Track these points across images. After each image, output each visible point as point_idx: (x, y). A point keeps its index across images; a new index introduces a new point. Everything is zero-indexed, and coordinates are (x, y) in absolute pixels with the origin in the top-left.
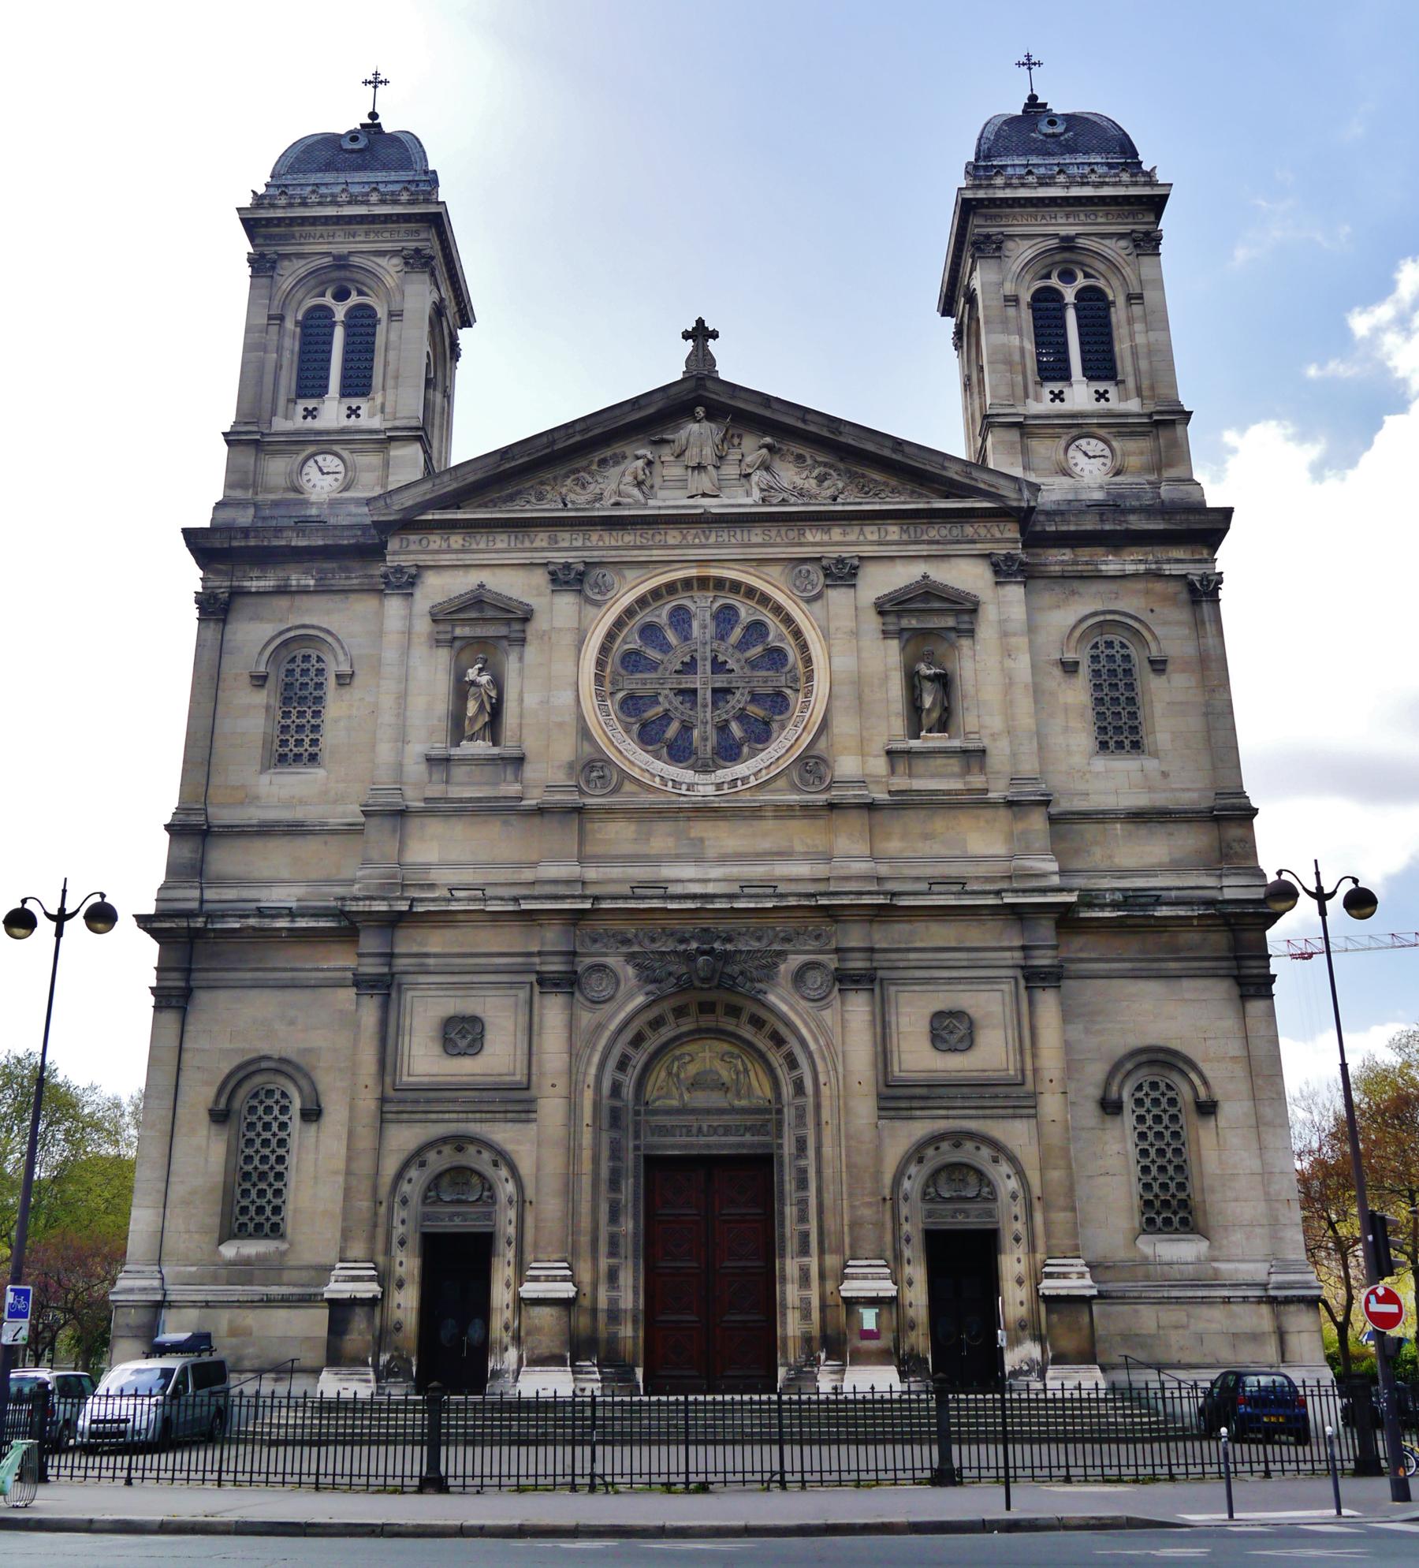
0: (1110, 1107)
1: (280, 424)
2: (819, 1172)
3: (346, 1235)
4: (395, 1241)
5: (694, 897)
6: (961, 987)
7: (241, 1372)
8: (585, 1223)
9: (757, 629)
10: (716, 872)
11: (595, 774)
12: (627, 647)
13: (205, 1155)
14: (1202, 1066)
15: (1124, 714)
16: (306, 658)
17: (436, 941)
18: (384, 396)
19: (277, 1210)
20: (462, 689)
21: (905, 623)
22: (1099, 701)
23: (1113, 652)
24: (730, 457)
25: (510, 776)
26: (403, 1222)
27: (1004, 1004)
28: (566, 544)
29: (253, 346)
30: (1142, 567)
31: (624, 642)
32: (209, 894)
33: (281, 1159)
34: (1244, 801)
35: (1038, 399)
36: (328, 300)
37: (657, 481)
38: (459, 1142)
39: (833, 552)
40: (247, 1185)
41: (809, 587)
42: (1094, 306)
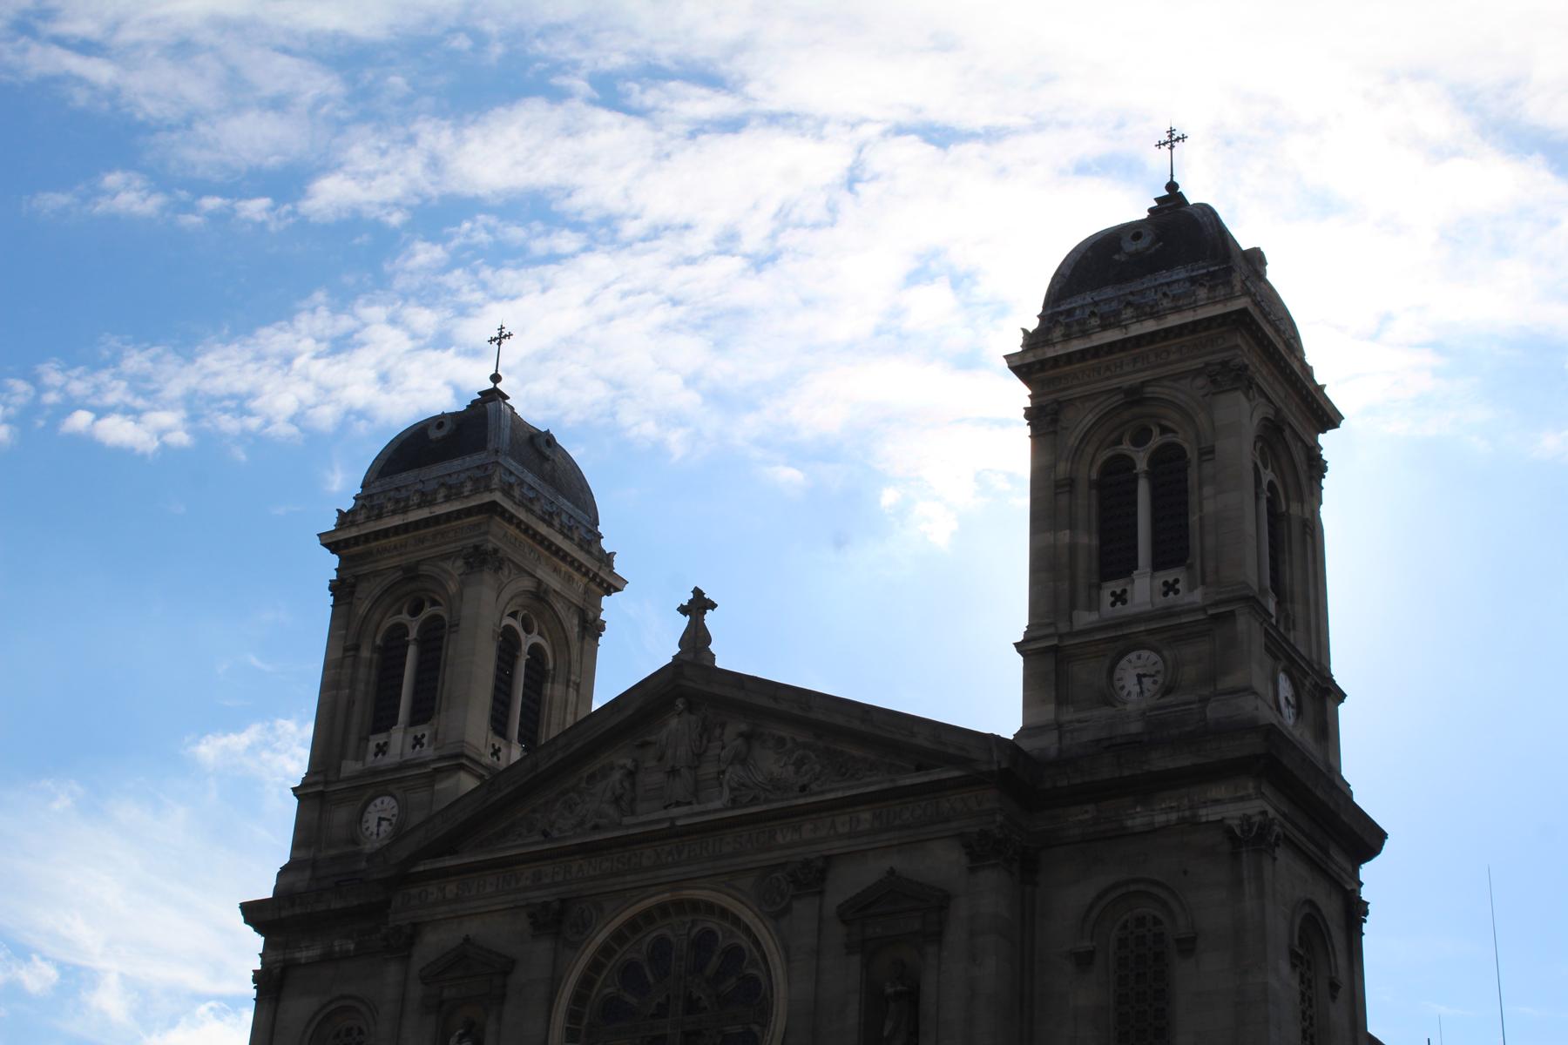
1: (350, 767)
28: (546, 881)
30: (1174, 816)
35: (1093, 605)
36: (404, 617)
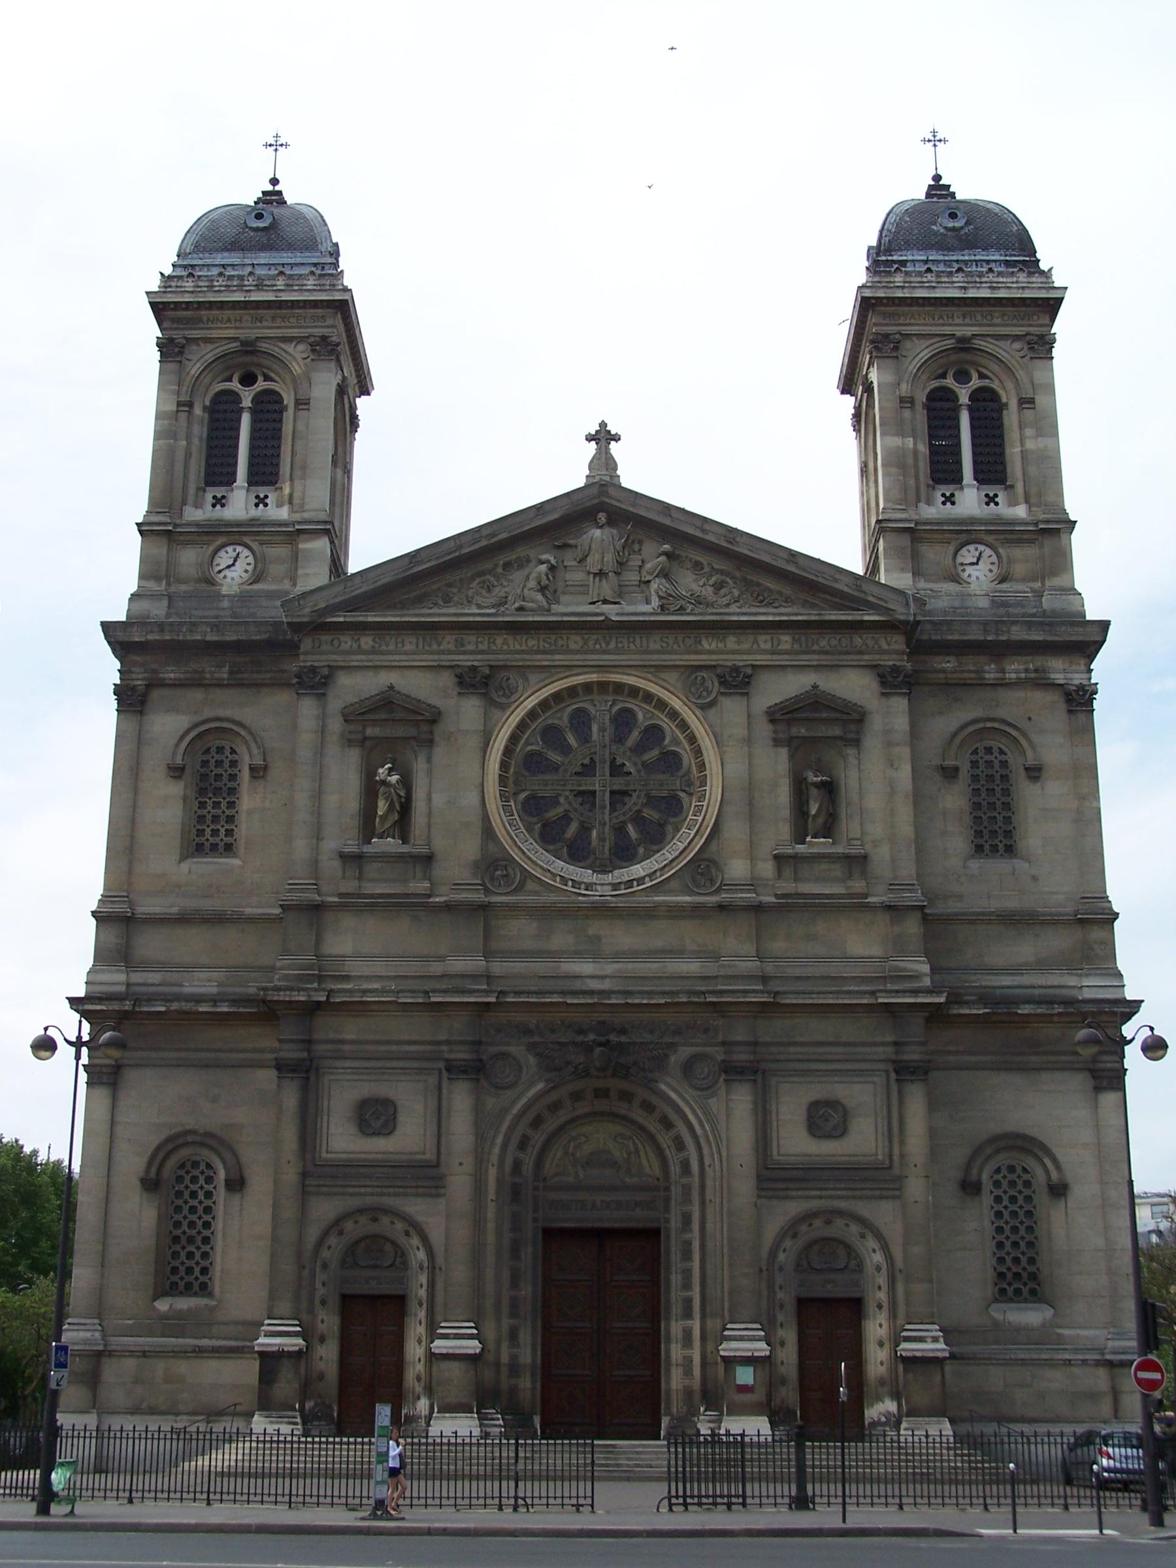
0: (970, 1187)
2: (703, 1246)
3: (273, 1296)
4: (317, 1301)
5: (592, 993)
6: (836, 1079)
7: (177, 1414)
8: (490, 1288)
9: (654, 733)
10: (610, 968)
11: (499, 873)
12: (530, 748)
13: (139, 1218)
14: (1055, 1151)
15: (999, 818)
16: (220, 750)
17: (351, 1029)
18: (292, 487)
19: (205, 1271)
20: (371, 789)
21: (794, 731)
22: (976, 806)
23: (992, 758)
24: (631, 563)
25: (419, 875)
26: (324, 1284)
27: (875, 1095)
28: (471, 647)
29: (166, 433)
31: (527, 743)
32: (136, 977)
33: (207, 1225)
34: (1107, 905)
36: (235, 385)
37: (560, 586)
38: (375, 1213)
39: (728, 660)
40: (178, 1248)
41: (705, 694)
42: (987, 409)
